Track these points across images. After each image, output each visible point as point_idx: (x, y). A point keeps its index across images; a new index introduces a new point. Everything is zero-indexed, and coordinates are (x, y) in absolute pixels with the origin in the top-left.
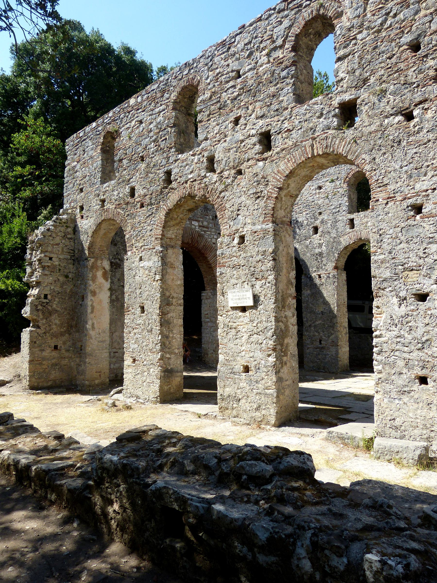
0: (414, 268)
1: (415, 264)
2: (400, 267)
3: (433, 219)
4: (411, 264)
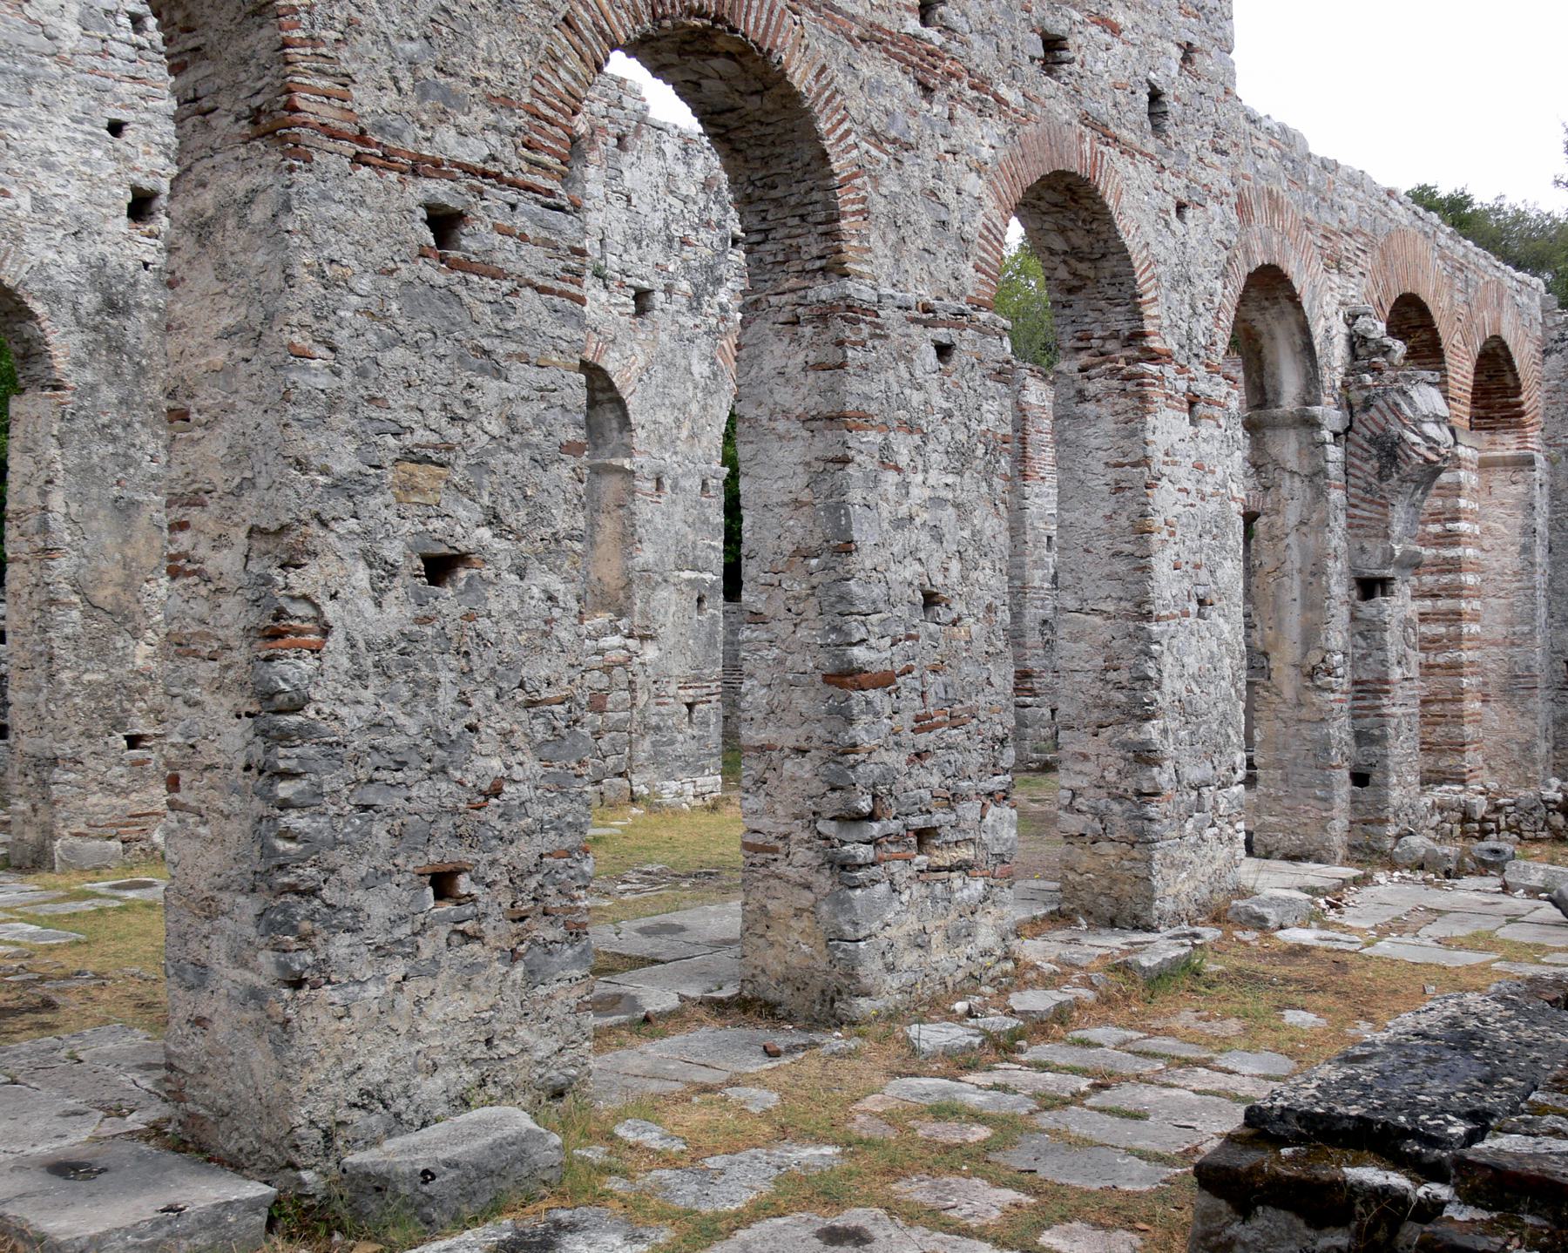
0: (430, 453)
1: (434, 438)
2: (391, 441)
3: (492, 283)
4: (421, 436)
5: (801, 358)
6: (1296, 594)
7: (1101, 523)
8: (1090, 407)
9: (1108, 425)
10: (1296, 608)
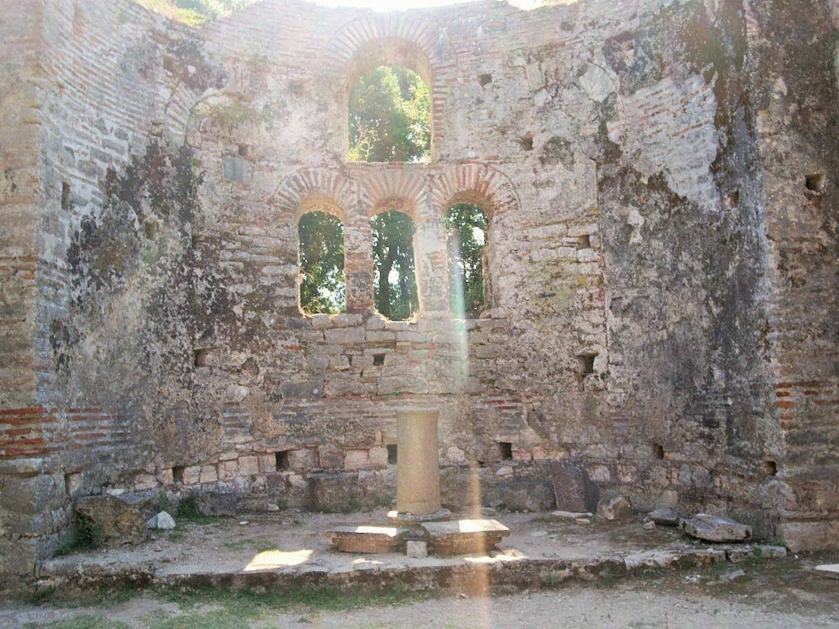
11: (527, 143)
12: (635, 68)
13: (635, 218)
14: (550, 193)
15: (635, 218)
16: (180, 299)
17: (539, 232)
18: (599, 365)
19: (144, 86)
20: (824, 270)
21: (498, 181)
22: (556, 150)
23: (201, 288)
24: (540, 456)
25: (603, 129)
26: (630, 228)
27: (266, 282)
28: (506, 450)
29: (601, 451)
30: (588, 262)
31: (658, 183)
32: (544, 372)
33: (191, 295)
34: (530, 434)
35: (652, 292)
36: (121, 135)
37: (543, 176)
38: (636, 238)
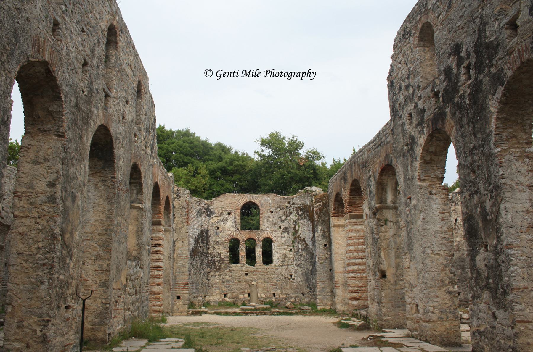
5: (526, 168)
6: (393, 254)
7: (439, 229)
8: (434, 197)
9: (439, 201)
10: (394, 258)
11: (280, 227)
12: (301, 215)
13: (300, 247)
14: (284, 239)
15: (300, 247)
16: (206, 261)
17: (283, 247)
18: (293, 277)
19: (200, 219)
20: (327, 261)
21: (274, 235)
22: (286, 230)
23: (210, 259)
24: (281, 296)
25: (295, 227)
26: (299, 249)
27: (223, 257)
28: (274, 294)
29: (292, 295)
30: (291, 255)
31: (304, 240)
32: (282, 278)
33: (208, 260)
34: (279, 292)
35: (303, 262)
36: (197, 229)
37: (283, 235)
38: (300, 251)
